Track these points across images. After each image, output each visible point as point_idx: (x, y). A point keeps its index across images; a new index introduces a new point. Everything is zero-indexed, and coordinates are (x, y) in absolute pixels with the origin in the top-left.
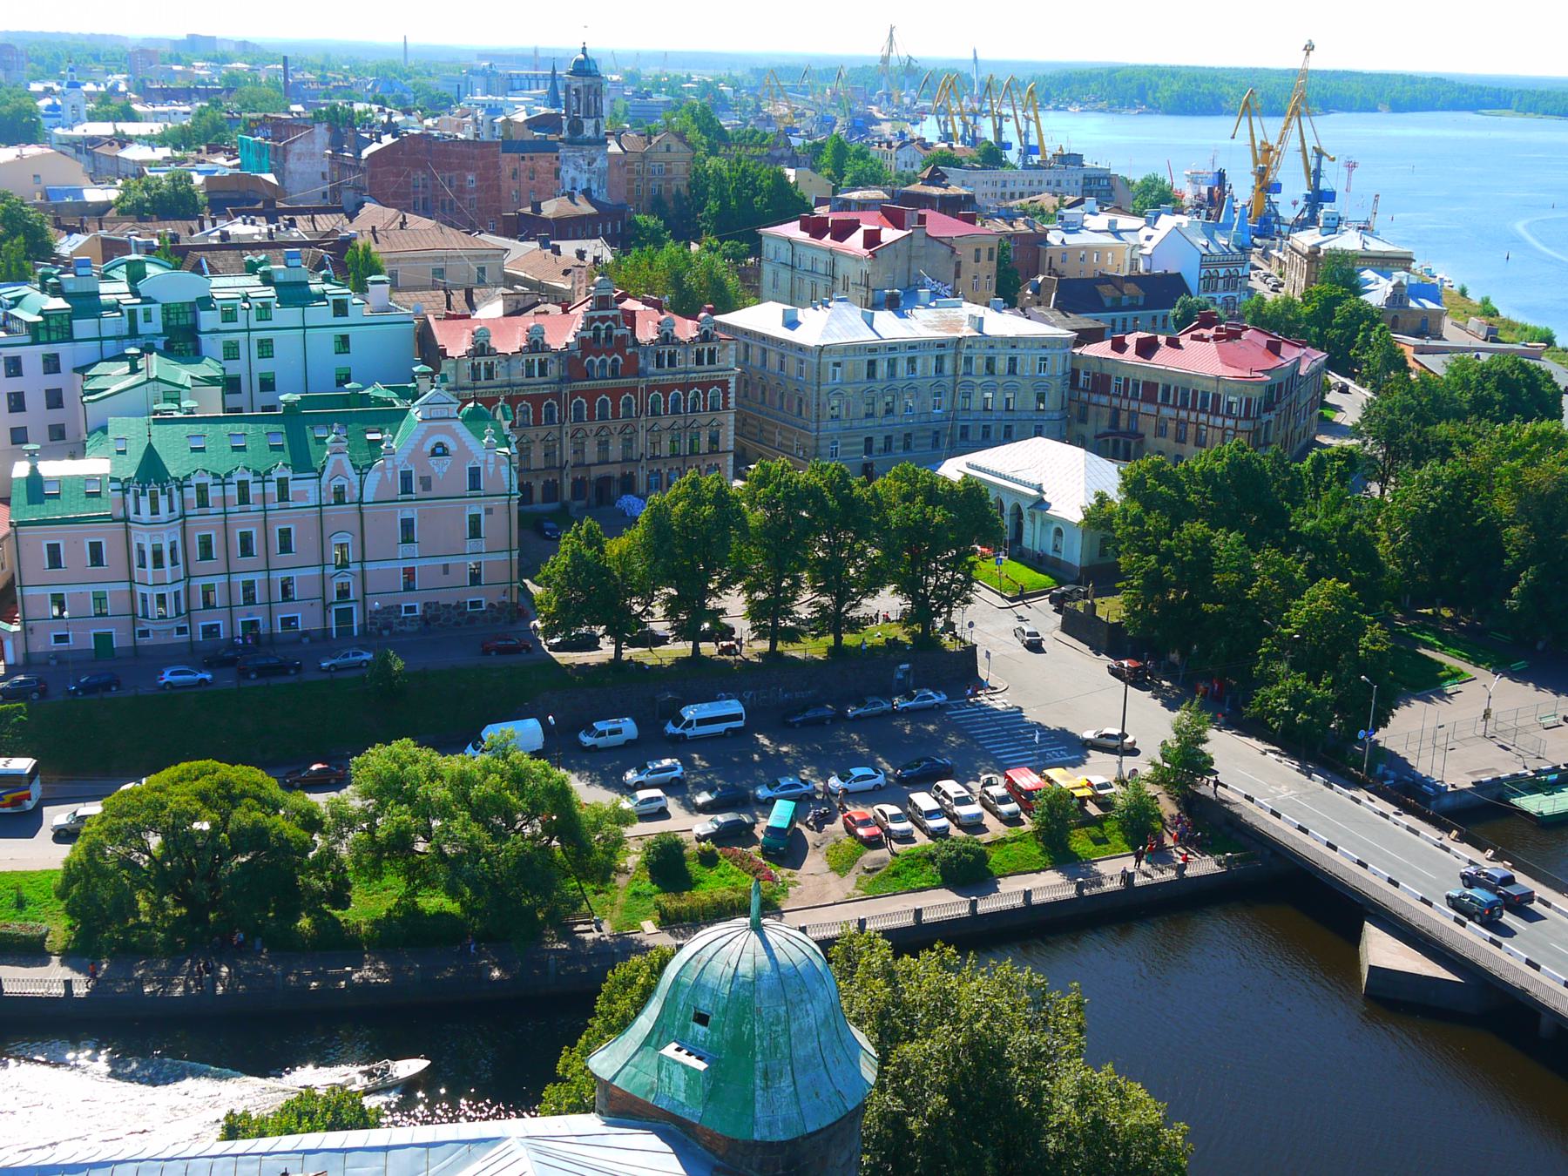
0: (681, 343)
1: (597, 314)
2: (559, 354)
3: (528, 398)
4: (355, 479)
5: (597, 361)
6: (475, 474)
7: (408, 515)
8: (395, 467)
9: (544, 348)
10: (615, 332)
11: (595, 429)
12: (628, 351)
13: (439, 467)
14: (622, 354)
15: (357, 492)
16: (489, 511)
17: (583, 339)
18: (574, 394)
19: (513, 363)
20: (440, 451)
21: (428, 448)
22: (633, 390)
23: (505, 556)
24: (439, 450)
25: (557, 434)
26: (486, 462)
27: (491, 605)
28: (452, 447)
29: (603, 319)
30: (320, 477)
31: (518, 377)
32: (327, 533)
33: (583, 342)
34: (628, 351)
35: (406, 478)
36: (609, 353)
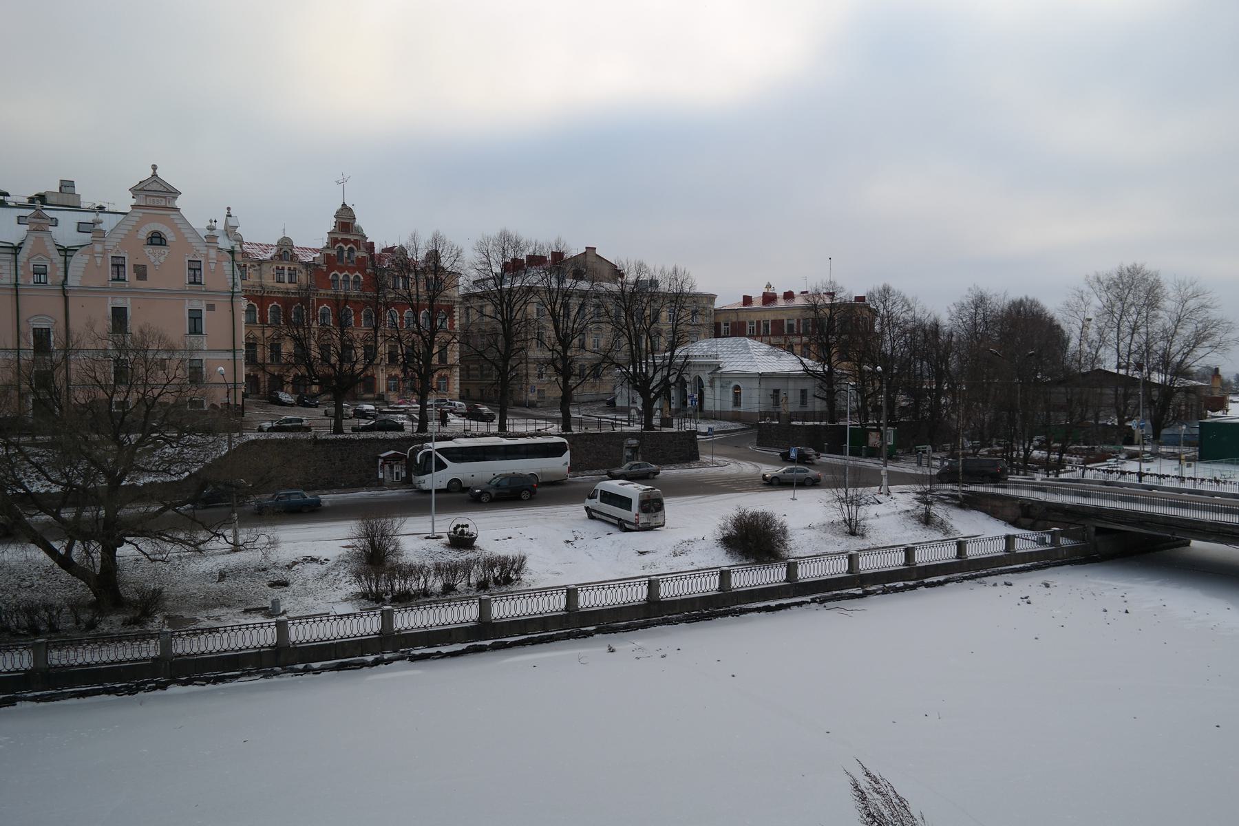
1: (340, 237)
2: (307, 265)
4: (59, 259)
5: (341, 276)
6: (195, 268)
7: (120, 303)
8: (105, 252)
9: (293, 257)
10: (356, 254)
13: (153, 256)
15: (61, 274)
16: (211, 307)
18: (320, 302)
19: (265, 267)
20: (156, 239)
21: (143, 234)
23: (230, 356)
24: (156, 241)
26: (207, 256)
27: (213, 406)
28: (170, 236)
30: (16, 254)
31: (269, 280)
32: (23, 318)
35: (118, 266)
36: (352, 270)
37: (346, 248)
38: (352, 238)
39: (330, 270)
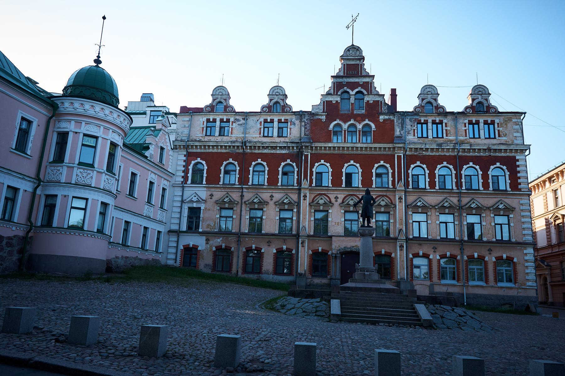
0: (446, 114)
2: (301, 114)
3: (264, 157)
5: (345, 126)
9: (286, 109)
10: (366, 99)
11: (341, 197)
12: (382, 118)
14: (376, 121)
17: (329, 103)
18: (316, 158)
19: (252, 121)
22: (389, 159)
25: (295, 197)
29: (353, 86)
33: (330, 108)
34: (382, 118)
37: (352, 93)
38: (361, 80)
39: (330, 119)
